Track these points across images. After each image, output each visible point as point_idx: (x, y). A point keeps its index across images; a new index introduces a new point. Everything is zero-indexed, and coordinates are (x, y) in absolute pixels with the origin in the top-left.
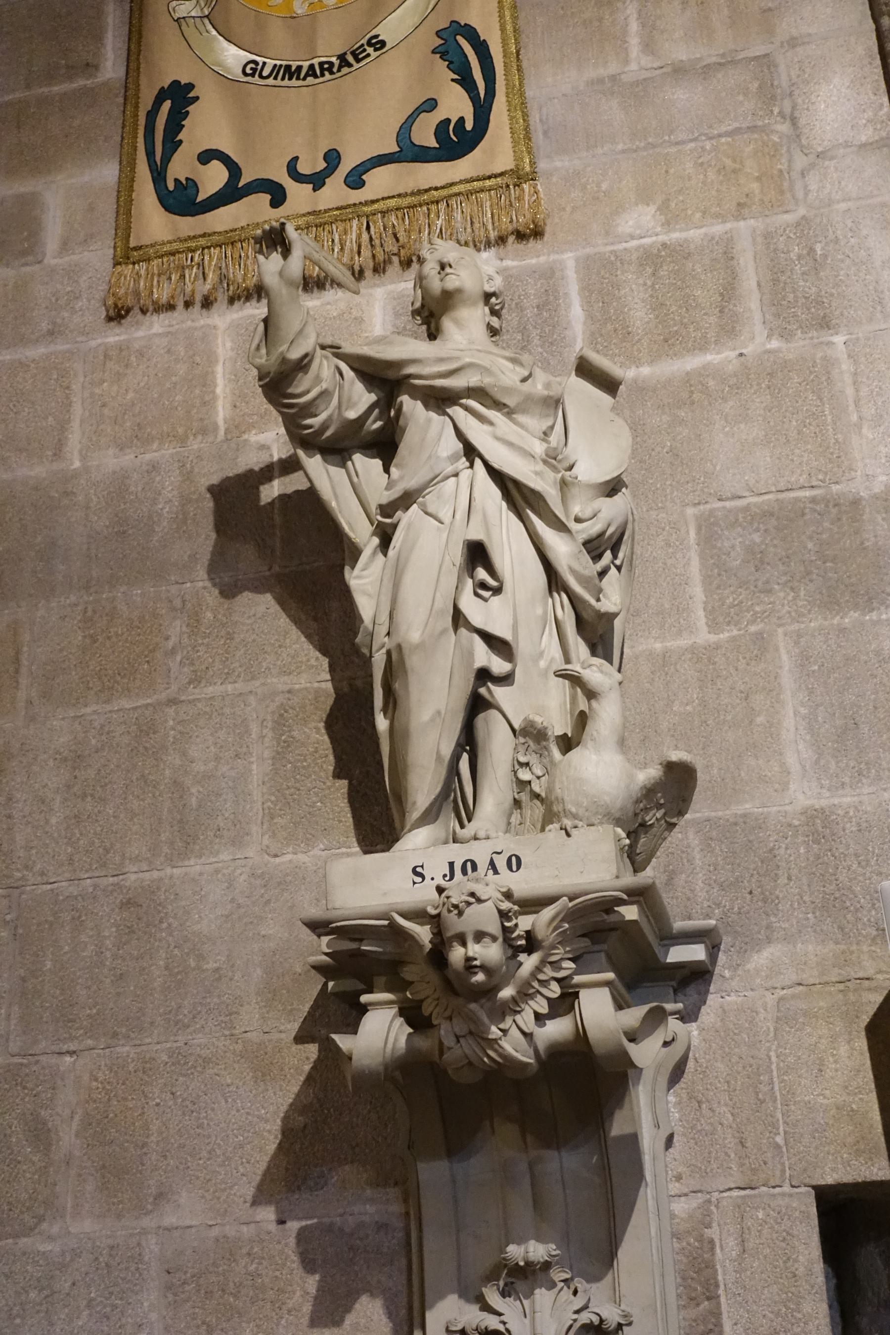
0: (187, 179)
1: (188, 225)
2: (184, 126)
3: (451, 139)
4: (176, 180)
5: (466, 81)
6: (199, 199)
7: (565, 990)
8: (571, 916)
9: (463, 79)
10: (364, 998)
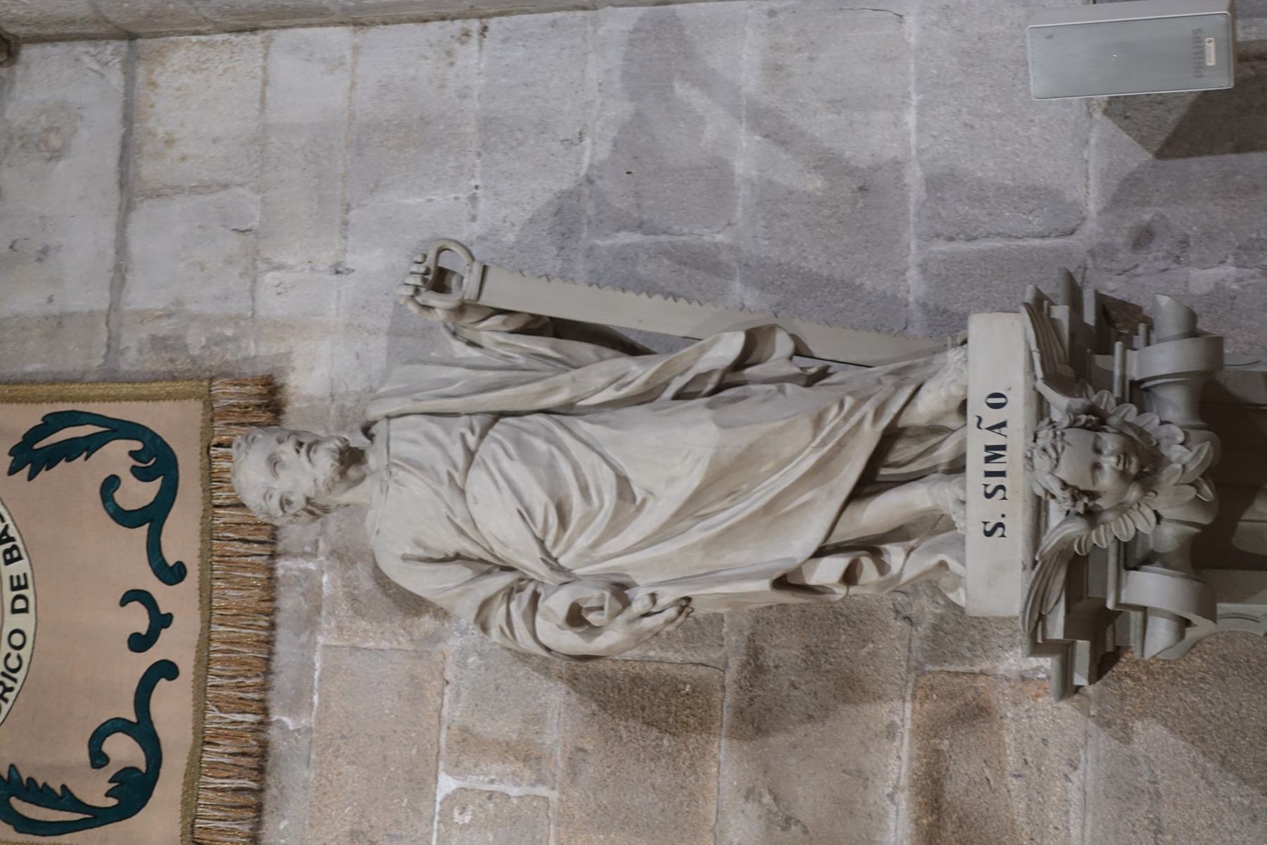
0: (111, 781)
1: (168, 789)
2: (45, 784)
3: (153, 464)
4: (108, 795)
5: (89, 446)
6: (143, 768)
7: (1127, 399)
8: (1053, 380)
9: (87, 449)
10: (1110, 605)
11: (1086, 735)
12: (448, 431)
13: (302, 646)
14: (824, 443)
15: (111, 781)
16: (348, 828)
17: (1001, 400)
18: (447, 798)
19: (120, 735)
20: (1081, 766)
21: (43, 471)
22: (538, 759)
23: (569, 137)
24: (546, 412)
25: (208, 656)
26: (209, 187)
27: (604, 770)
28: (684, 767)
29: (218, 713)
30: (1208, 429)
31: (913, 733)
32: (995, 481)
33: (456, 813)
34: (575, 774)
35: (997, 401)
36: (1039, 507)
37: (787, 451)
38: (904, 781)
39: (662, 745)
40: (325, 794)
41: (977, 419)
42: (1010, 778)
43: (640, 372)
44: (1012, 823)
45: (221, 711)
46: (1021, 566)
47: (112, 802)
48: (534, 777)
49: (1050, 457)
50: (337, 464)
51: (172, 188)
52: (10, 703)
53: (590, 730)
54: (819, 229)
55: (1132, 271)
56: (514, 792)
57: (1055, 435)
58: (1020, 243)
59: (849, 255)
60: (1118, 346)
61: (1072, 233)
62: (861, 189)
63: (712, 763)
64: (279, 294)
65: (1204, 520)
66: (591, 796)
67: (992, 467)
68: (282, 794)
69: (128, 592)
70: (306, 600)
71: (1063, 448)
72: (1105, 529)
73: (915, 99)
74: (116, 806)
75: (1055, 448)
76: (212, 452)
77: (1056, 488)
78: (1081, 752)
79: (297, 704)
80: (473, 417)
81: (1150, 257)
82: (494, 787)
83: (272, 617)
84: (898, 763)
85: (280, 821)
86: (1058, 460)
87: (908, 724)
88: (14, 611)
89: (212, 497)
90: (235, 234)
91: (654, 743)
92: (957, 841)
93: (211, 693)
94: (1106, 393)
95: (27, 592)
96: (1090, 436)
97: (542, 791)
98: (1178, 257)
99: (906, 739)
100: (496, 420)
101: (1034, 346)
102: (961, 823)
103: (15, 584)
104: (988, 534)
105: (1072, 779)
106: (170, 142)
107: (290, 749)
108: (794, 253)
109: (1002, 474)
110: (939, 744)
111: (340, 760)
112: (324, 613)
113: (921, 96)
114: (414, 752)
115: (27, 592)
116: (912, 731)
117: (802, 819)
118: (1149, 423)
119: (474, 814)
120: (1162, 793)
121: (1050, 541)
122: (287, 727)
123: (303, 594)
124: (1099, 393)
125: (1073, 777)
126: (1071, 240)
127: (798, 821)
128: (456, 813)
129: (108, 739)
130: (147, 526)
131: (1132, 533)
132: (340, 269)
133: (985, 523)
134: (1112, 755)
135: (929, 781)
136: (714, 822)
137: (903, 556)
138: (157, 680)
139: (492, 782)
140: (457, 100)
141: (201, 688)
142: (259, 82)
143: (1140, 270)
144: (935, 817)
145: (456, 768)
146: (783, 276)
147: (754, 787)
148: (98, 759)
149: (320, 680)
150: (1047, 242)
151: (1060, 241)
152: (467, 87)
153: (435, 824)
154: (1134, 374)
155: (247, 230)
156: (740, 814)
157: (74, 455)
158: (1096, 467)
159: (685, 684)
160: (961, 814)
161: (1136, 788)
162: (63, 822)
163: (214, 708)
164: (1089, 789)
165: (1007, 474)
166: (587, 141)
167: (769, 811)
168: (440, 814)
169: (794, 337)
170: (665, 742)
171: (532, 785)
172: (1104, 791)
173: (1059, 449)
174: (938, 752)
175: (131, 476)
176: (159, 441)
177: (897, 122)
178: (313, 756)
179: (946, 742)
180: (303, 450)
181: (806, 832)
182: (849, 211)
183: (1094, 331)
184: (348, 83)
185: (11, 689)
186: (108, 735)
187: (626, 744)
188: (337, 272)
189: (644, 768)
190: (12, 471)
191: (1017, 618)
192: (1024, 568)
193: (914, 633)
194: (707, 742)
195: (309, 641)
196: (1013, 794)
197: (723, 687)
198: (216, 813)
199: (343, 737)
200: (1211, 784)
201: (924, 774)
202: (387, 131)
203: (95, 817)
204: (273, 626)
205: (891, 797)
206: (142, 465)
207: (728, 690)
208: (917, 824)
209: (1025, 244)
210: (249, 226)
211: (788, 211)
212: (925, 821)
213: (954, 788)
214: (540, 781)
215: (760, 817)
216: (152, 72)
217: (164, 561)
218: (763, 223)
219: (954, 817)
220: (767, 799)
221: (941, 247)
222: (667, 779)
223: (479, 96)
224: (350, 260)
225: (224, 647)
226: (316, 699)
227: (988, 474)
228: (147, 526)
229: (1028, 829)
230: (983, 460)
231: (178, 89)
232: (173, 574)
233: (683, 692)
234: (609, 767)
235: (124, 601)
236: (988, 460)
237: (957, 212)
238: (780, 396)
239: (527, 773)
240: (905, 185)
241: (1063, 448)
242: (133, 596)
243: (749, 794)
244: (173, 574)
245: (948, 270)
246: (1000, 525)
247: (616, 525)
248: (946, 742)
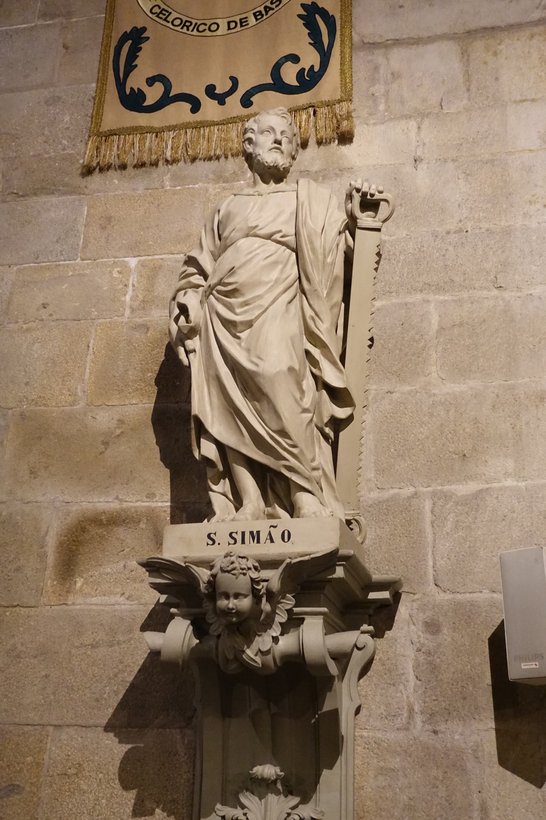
0: (138, 89)
4: (132, 89)
11: (145, 604)
12: (287, 222)
13: (207, 176)
14: (272, 437)
15: (138, 89)
16: (112, 215)
17: (286, 539)
18: (127, 263)
19: (163, 89)
20: (129, 602)
21: (303, 22)
22: (144, 308)
23: (498, 281)
24: (300, 278)
26: (468, 81)
27: (137, 343)
28: (137, 386)
29: (172, 136)
31: (148, 508)
32: (239, 537)
33: (119, 269)
34: (135, 328)
37: (266, 417)
38: (125, 505)
39: (148, 373)
40: (130, 200)
41: (275, 525)
42: (123, 562)
43: (321, 329)
44: (100, 565)
45: (173, 138)
46: (186, 555)
48: (135, 307)
49: (228, 566)
51: (468, 60)
52: (181, 30)
53: (158, 333)
54: (439, 433)
55: (411, 622)
56: (128, 298)
57: (242, 569)
58: (430, 553)
59: (423, 452)
61: (436, 585)
62: (465, 455)
63: (138, 400)
64: (403, 130)
66: (124, 338)
67: (247, 536)
68: (131, 178)
69: (237, 79)
70: (231, 174)
71: (233, 574)
73: (522, 484)
75: (234, 569)
76: (311, 109)
77: (214, 571)
78: (136, 602)
79: (175, 178)
80: (294, 236)
81: (420, 633)
82: (131, 287)
83: (223, 157)
84: (134, 500)
85: (117, 179)
86: (229, 572)
87: (154, 505)
88: (229, 23)
90: (439, 100)
91: (149, 368)
92: (93, 535)
94: (293, 602)
95: (239, 28)
97: (127, 312)
98: (420, 650)
99: (147, 504)
100: (293, 250)
101: (312, 556)
102: (102, 537)
103: (243, 21)
104: (209, 536)
105: (122, 597)
106: (495, 54)
107: (154, 179)
108: (424, 419)
109: (243, 542)
110: (144, 523)
111: (148, 205)
112: (224, 185)
113: (524, 488)
114: (150, 243)
115: (239, 28)
116: (150, 507)
117: (107, 451)
118: (274, 630)
119: (116, 279)
120: (113, 648)
122: (165, 176)
123: (234, 172)
124: (292, 598)
125: (122, 598)
126: (432, 585)
127: (106, 449)
128: (119, 269)
129: (161, 84)
131: (210, 621)
132: (418, 162)
133: (215, 534)
134: (133, 619)
135: (124, 518)
136: (107, 404)
137: (221, 491)
138: (190, 103)
139: (133, 286)
140: (521, 213)
141: (185, 126)
142: (533, 96)
143: (412, 627)
144: (105, 522)
145: (143, 265)
146: (410, 414)
147: (125, 424)
148: (151, 81)
149: (189, 188)
150: (431, 571)
151: (431, 577)
152: (530, 217)
153: (113, 259)
155: (442, 106)
156: (111, 418)
157: (312, 37)
158: (227, 597)
159: (180, 382)
160: (107, 537)
161: (116, 633)
162: (119, 69)
163: (175, 134)
164: (117, 607)
165: (243, 545)
166: (495, 292)
167: (112, 433)
168: (118, 261)
169: (350, 418)
170: (150, 374)
171: (131, 307)
172: (115, 615)
173: (233, 572)
174: (139, 522)
175: (299, 69)
177: (507, 474)
178: (150, 191)
179: (144, 526)
180: (276, 145)
181: (101, 453)
182: (451, 450)
184: (533, 148)
185: (188, 30)
186: (163, 84)
187: (150, 353)
188: (415, 161)
189: (137, 364)
190: (303, 5)
191: (162, 555)
192: (185, 557)
193: (204, 505)
194: (149, 396)
195: (209, 179)
196: (115, 565)
197: (177, 402)
198: (121, 145)
199: (159, 205)
200: (116, 676)
201: (128, 515)
202: (502, 175)
203: (121, 85)
204: (218, 158)
205: (117, 498)
207: (176, 405)
208: (102, 513)
209: (429, 556)
210: (444, 107)
211: (451, 413)
212: (103, 517)
213: (120, 532)
214: (133, 310)
215: (109, 428)
216: (540, 35)
217: (254, 95)
218: (443, 400)
219: (105, 533)
220: (118, 432)
221: (428, 506)
222: (131, 377)
223: (524, 225)
224: (422, 166)
226: (179, 188)
227: (243, 533)
229: (97, 573)
230: (251, 530)
233: (176, 381)
234: (138, 346)
235: (232, 78)
236: (251, 533)
237: (449, 514)
238: (301, 410)
239: (137, 303)
240: (467, 482)
241: (233, 574)
242: (235, 81)
243: (121, 422)
245: (413, 511)
246: (214, 542)
247: (229, 324)
248: (144, 526)
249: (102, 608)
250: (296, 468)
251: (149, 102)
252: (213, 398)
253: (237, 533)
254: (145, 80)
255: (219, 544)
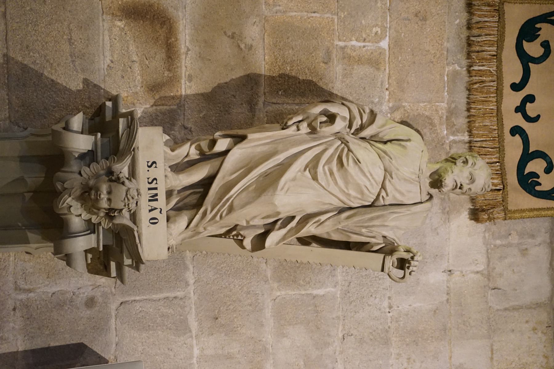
0: (539, 35)
4: (540, 29)
6: (524, 42)
11: (104, 81)
12: (394, 197)
13: (453, 102)
14: (228, 200)
15: (539, 35)
16: (428, 22)
17: (151, 221)
20: (106, 67)
22: (344, 58)
23: (349, 337)
24: (351, 208)
25: (497, 95)
26: (514, 309)
27: (315, 55)
28: (280, 58)
29: (491, 69)
30: (60, 214)
32: (153, 186)
33: (379, 32)
34: (328, 52)
35: (154, 221)
36: (133, 174)
37: (244, 195)
40: (439, 37)
43: (310, 228)
44: (135, 41)
45: (490, 70)
47: (538, 26)
48: (346, 50)
50: (443, 180)
51: (531, 308)
53: (322, 72)
54: (234, 299)
55: (94, 287)
56: (354, 43)
57: (128, 205)
58: (145, 297)
59: (220, 288)
60: (101, 249)
61: (122, 303)
64: (477, 260)
65: (60, 174)
66: (320, 43)
70: (453, 123)
71: (125, 199)
72: (103, 167)
73: (194, 361)
74: (536, 24)
75: (128, 199)
76: (502, 186)
77: (127, 182)
78: (106, 73)
81: (86, 294)
82: (362, 44)
83: (469, 114)
84: (186, 65)
85: (459, 23)
86: (127, 194)
87: (183, 81)
89: (500, 166)
90: (499, 287)
91: (294, 68)
92: (159, 32)
93: (495, 78)
94: (106, 227)
96: (113, 206)
97: (341, 44)
99: (183, 75)
100: (373, 203)
101: (139, 245)
104: (154, 162)
106: (534, 329)
109: (149, 189)
110: (169, 74)
111: (433, 52)
112: (445, 117)
113: (192, 362)
114: (400, 58)
116: (181, 79)
117: (227, 38)
119: (371, 31)
120: (69, 57)
121: (128, 161)
122: (458, 65)
123: (455, 125)
125: (109, 62)
127: (229, 37)
128: (379, 32)
129: (542, 54)
130: (530, 152)
131: (91, 166)
132: (449, 273)
133: (156, 167)
134: (92, 72)
135: (172, 57)
136: (265, 35)
137: (190, 153)
138: (520, 82)
139: (364, 47)
140: (401, 352)
141: (499, 79)
142: (495, 359)
143: (91, 288)
144: (169, 42)
145: (381, 52)
146: (249, 277)
147: (249, 51)
149: (444, 87)
150: (133, 298)
151: (127, 299)
152: (398, 359)
154: (93, 236)
155: (494, 289)
156: (254, 38)
158: (109, 193)
159: (281, 94)
160: (157, 44)
161: (81, 58)
163: (493, 71)
164: (102, 57)
166: (341, 335)
167: (241, 41)
169: (243, 247)
170: (289, 69)
171: (346, 46)
172: (95, 57)
173: (126, 198)
174: (169, 70)
175: (539, 174)
176: (528, 190)
177: (203, 349)
178: (446, 53)
179: (166, 75)
180: (459, 185)
181: (225, 33)
182: (221, 308)
183: (111, 258)
184: (453, 359)
186: (541, 56)
188: (450, 271)
189: (298, 57)
191: (140, 126)
192: (138, 148)
193: (182, 122)
194: (270, 69)
195: (451, 104)
196: (135, 53)
197: (265, 94)
198: (489, 24)
199: (432, 62)
201: (175, 60)
202: (432, 337)
204: (468, 110)
205: (188, 50)
206: (534, 179)
208: (177, 38)
209: (142, 297)
210: (493, 291)
212: (173, 39)
213: (161, 55)
214: (343, 48)
215: (245, 38)
216: (547, 363)
217: (521, 136)
218: (259, 301)
219: (160, 42)
220: (243, 46)
221: (180, 294)
222: (287, 53)
223: (391, 355)
224: (445, 277)
225: (490, 99)
226: (446, 79)
227: (156, 189)
228: (530, 152)
231: (533, 355)
232: (516, 131)
233: (282, 91)
234: (313, 56)
235: (538, 117)
236: (156, 195)
237: (173, 310)
238: (248, 220)
239: (349, 51)
240: (197, 321)
241: (125, 199)
242: (536, 119)
243: (251, 47)
244: (516, 131)
247: (317, 159)
248: (166, 75)
249: (101, 44)
250: (205, 218)
251: (526, 45)
252: (260, 147)
253: (156, 183)
254: (547, 40)
255: (148, 171)
